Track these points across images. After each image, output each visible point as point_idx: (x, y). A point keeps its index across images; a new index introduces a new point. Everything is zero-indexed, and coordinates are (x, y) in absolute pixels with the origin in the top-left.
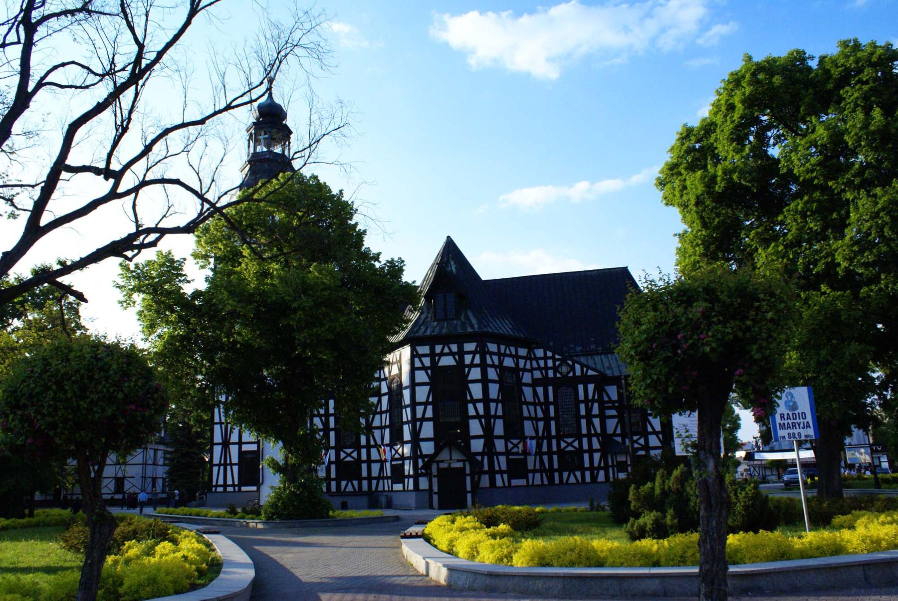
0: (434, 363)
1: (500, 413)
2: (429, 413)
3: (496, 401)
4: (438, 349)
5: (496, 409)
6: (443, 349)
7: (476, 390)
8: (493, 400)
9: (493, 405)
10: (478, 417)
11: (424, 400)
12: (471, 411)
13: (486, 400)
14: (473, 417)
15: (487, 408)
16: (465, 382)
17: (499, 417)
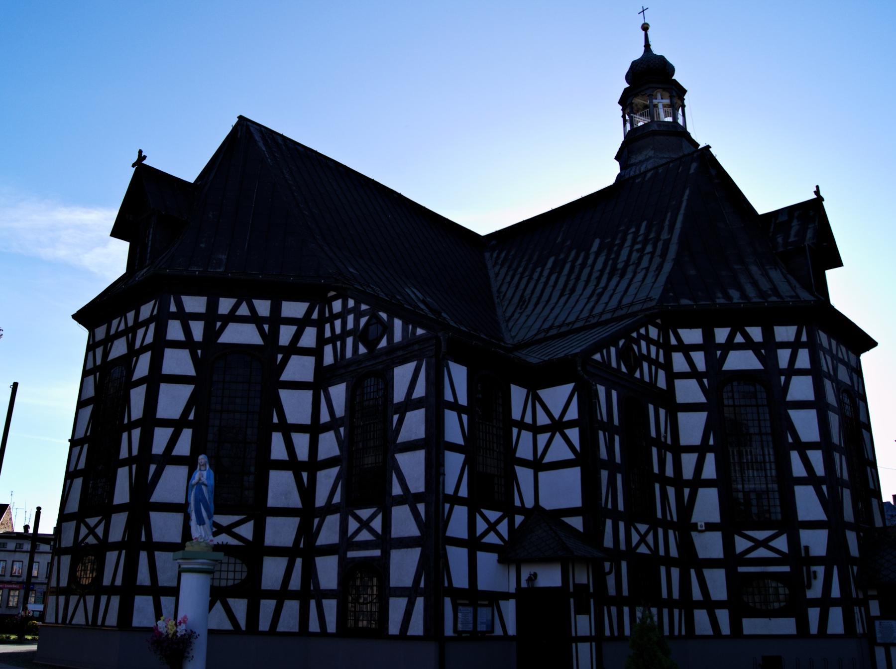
2: (710, 471)
10: (811, 479)
12: (798, 469)
16: (780, 407)
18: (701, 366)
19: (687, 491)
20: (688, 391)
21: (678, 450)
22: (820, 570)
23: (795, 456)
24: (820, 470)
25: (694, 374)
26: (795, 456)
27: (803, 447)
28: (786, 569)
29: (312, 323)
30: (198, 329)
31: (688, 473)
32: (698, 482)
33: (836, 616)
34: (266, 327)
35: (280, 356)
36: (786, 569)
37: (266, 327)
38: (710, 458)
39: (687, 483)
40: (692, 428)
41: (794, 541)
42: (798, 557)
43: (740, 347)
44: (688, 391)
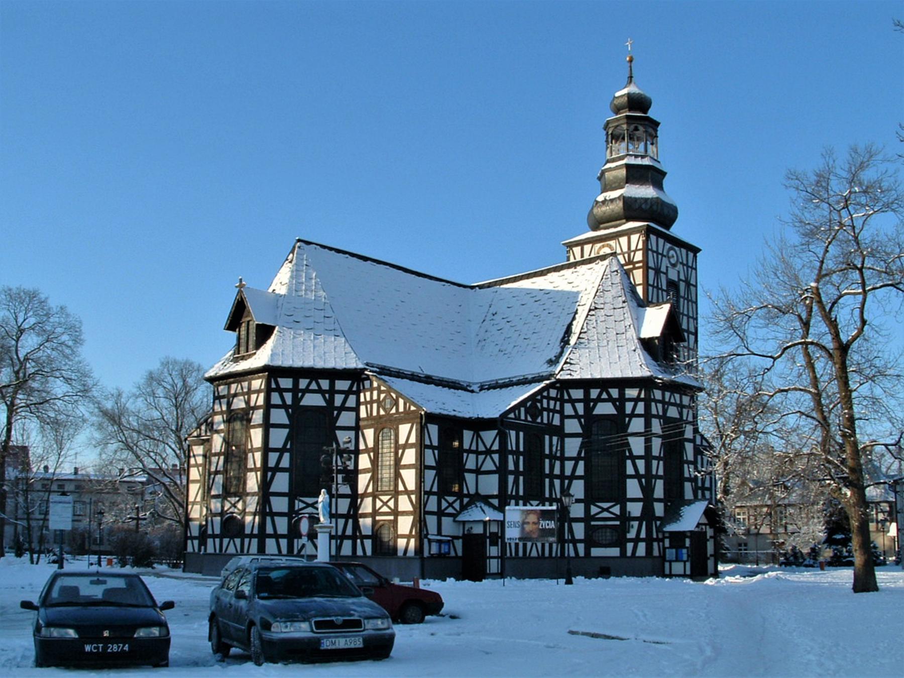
0: (588, 410)
1: (661, 472)
2: (580, 471)
3: (658, 458)
4: (594, 393)
5: (658, 468)
6: (600, 394)
7: (637, 446)
8: (655, 458)
9: (655, 463)
10: (637, 476)
11: (575, 454)
12: (630, 470)
13: (648, 456)
14: (631, 477)
15: (648, 467)
17: (660, 477)
18: (581, 412)
19: (567, 482)
20: (572, 426)
21: (563, 459)
22: (636, 524)
23: (629, 462)
24: (642, 471)
25: (576, 416)
26: (629, 462)
27: (633, 458)
28: (618, 523)
29: (353, 393)
30: (288, 397)
31: (568, 472)
32: (573, 477)
33: (642, 546)
34: (327, 396)
35: (335, 412)
36: (618, 523)
37: (327, 396)
38: (581, 464)
39: (567, 477)
40: (573, 447)
41: (623, 509)
42: (625, 518)
43: (604, 400)
44: (572, 426)
